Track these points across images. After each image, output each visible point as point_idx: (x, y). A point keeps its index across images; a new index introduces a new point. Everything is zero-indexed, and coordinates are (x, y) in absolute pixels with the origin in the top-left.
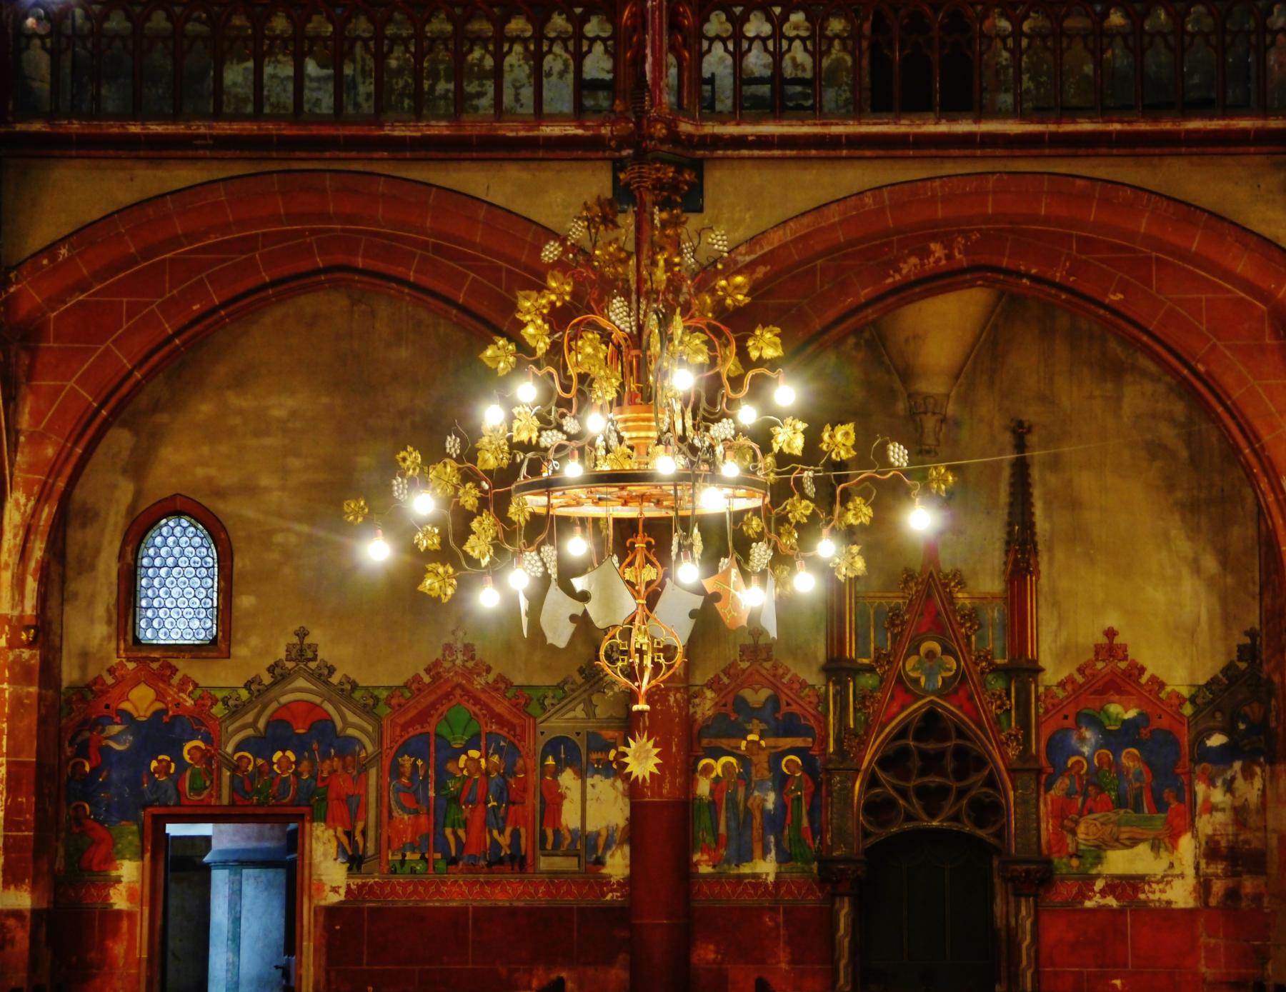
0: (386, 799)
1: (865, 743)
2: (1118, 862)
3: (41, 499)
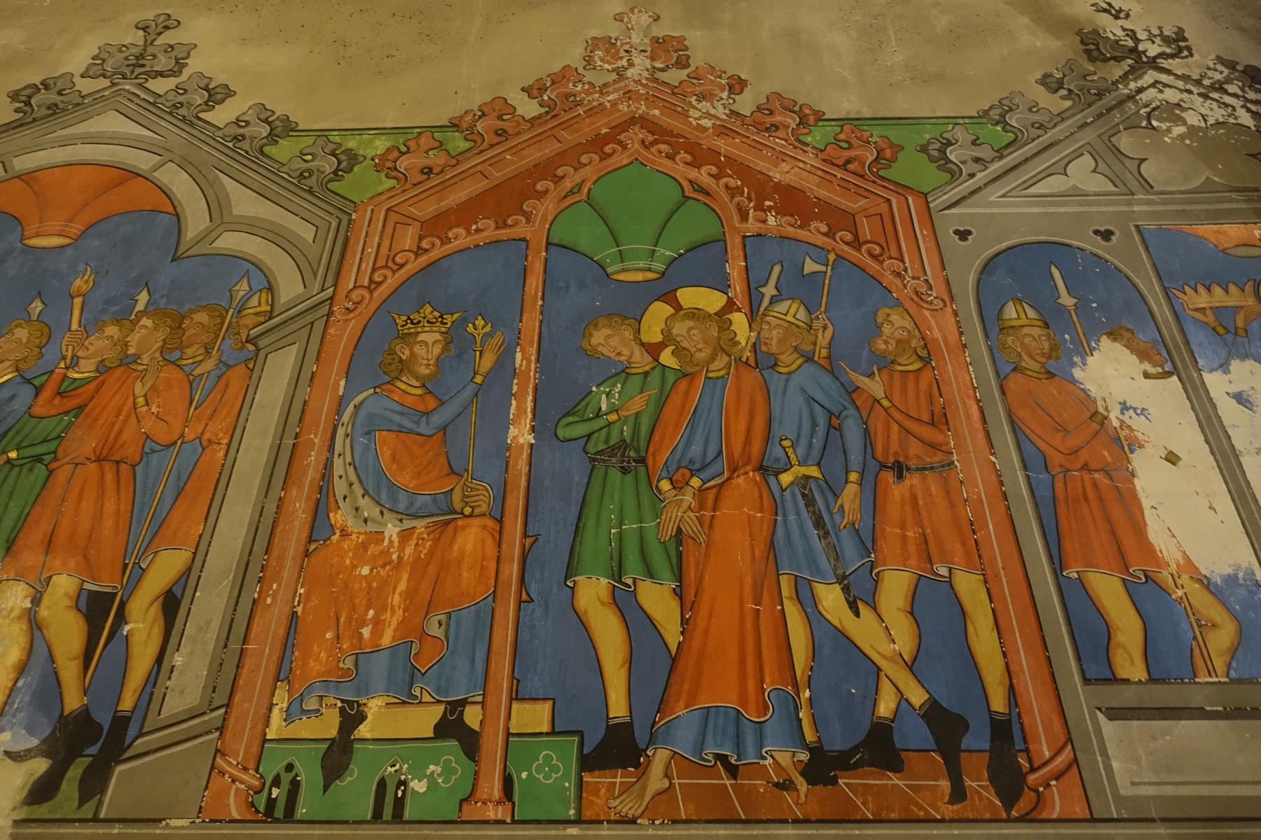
0: (314, 459)
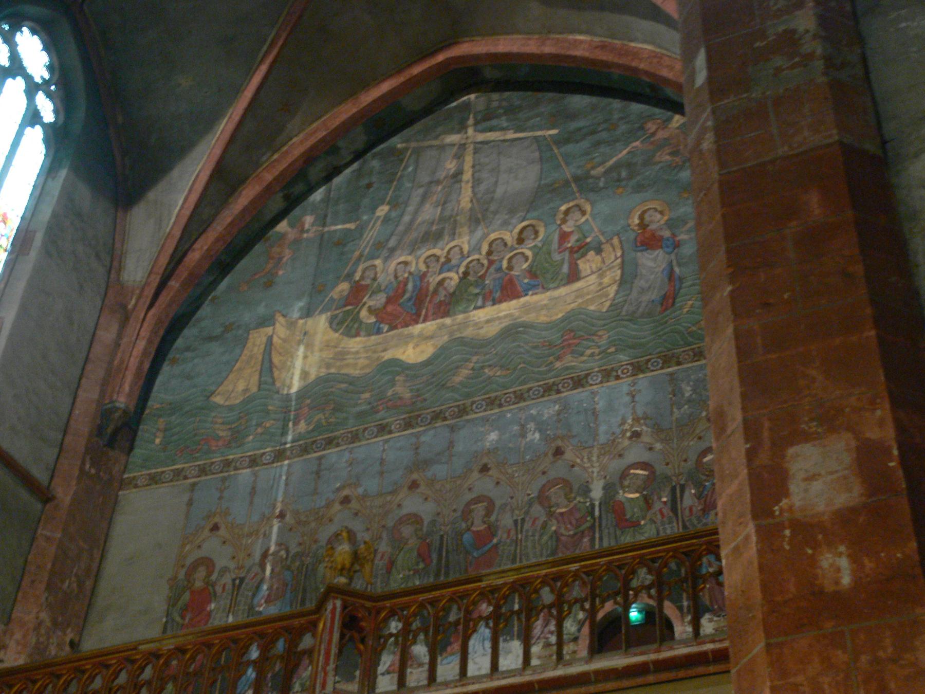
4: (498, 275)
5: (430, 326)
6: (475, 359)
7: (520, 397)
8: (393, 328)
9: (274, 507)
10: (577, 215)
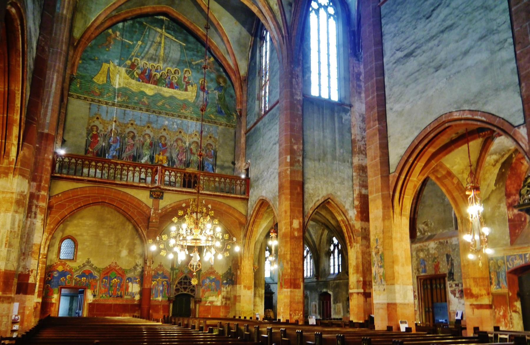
1: (176, 280)
2: (211, 299)
3: (50, 234)
4: (169, 80)
5: (153, 86)
6: (163, 101)
7: (173, 115)
8: (143, 82)
9: (113, 118)
10: (188, 73)
